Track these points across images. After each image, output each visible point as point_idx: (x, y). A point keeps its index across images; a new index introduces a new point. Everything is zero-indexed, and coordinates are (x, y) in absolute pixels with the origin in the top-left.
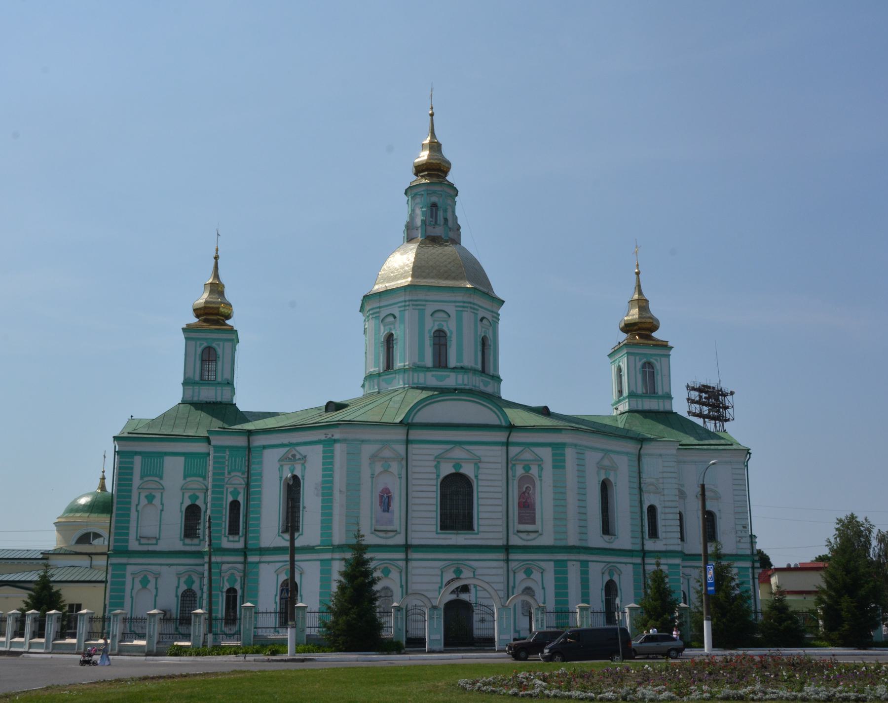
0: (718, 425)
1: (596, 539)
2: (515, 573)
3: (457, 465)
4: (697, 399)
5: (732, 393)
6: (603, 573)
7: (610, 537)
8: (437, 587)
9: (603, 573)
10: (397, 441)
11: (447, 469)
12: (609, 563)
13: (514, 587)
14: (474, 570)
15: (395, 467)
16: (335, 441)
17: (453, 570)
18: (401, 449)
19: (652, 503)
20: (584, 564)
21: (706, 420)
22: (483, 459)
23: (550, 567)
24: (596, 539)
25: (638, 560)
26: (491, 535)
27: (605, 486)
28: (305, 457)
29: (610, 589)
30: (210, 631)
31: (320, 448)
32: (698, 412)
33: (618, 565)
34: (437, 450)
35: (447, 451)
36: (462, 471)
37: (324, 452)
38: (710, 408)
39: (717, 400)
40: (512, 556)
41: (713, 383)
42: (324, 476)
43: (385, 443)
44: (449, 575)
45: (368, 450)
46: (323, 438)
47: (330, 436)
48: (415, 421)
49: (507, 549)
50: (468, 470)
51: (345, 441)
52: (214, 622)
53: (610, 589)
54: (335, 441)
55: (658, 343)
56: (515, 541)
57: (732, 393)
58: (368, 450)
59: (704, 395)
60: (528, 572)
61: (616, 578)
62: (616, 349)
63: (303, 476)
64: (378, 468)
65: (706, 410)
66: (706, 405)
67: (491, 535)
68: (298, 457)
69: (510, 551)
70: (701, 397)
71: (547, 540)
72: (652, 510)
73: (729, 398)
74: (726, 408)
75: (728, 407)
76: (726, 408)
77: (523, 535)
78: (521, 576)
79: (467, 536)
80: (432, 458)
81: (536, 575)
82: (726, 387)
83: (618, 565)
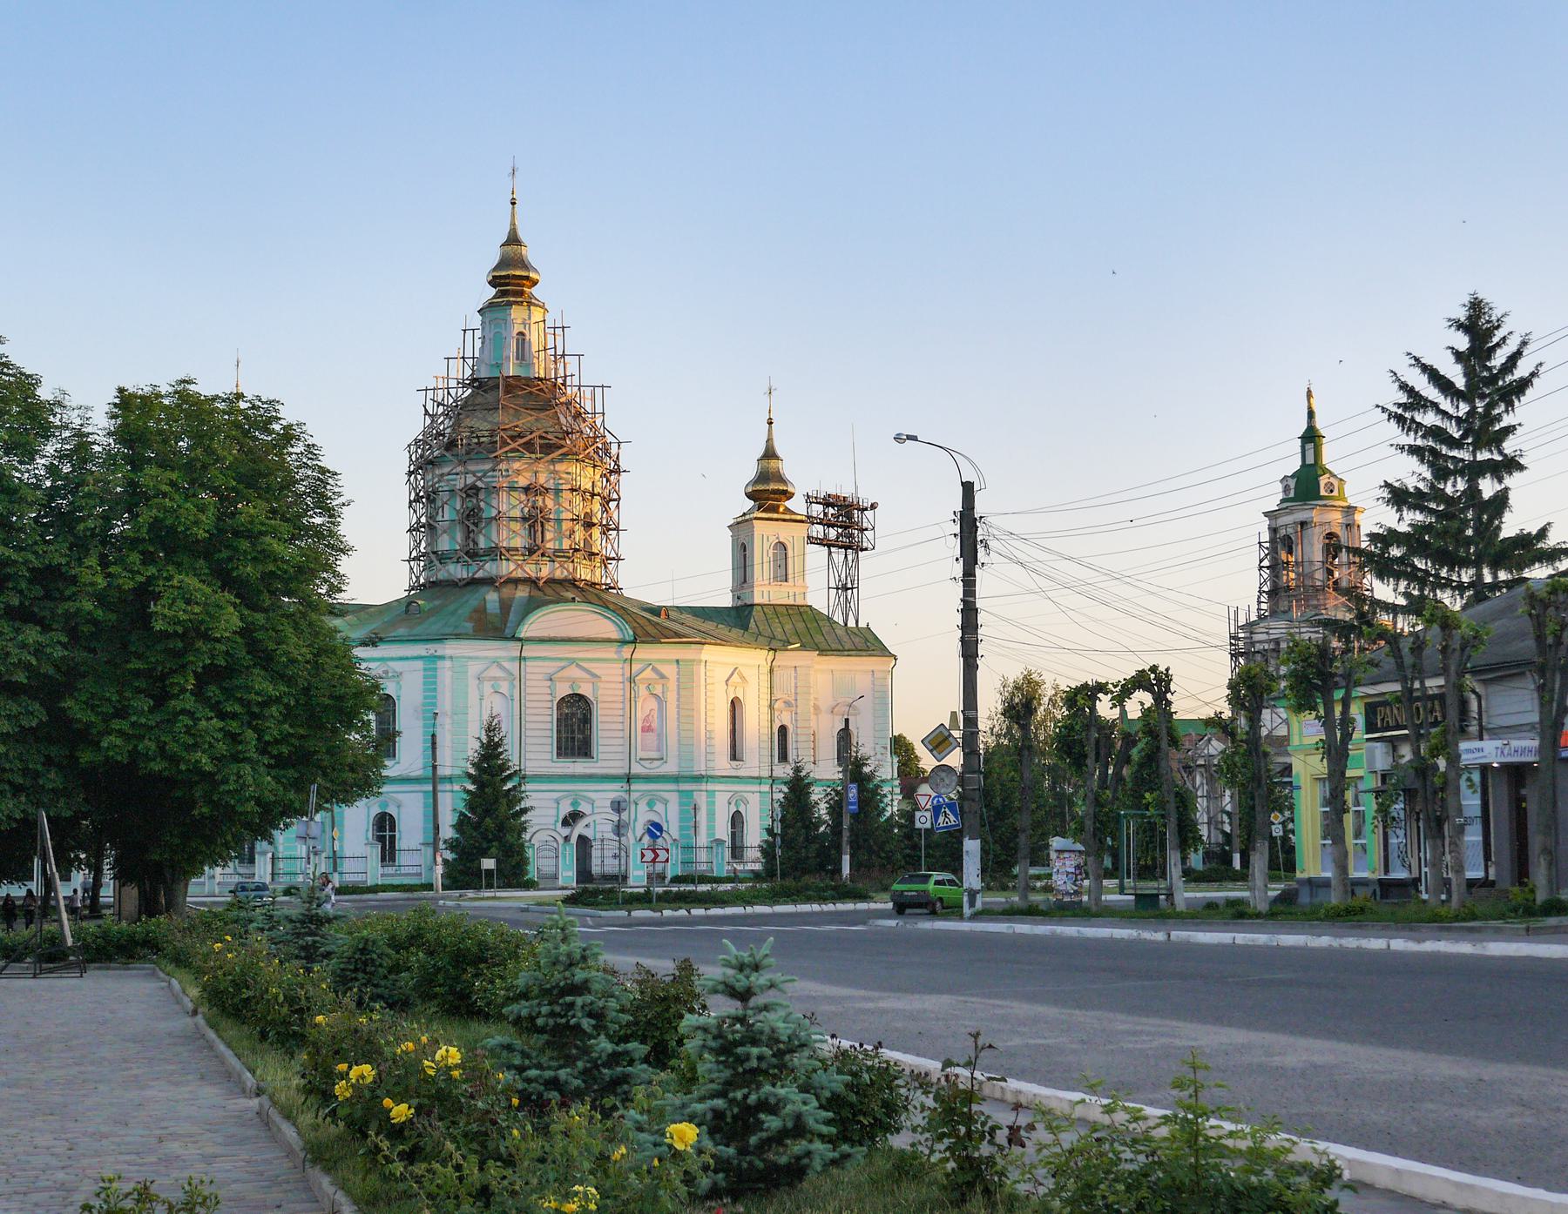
0: (850, 558)
1: (723, 764)
2: (636, 804)
3: (573, 682)
4: (822, 516)
5: (873, 507)
6: (730, 804)
7: (737, 763)
8: (552, 820)
9: (730, 804)
10: (513, 659)
11: (563, 690)
12: (737, 792)
13: (635, 820)
14: (592, 802)
15: (504, 687)
16: (442, 658)
17: (569, 802)
18: (513, 667)
19: (785, 723)
20: (711, 793)
21: (833, 549)
22: (603, 678)
23: (673, 798)
24: (723, 764)
25: (766, 788)
26: (611, 764)
27: (735, 704)
28: (401, 673)
29: (737, 820)
30: (335, 870)
31: (419, 664)
32: (821, 536)
33: (745, 795)
34: (550, 667)
35: (563, 668)
36: (580, 692)
37: (425, 670)
38: (840, 531)
39: (850, 516)
40: (633, 787)
41: (846, 491)
42: (425, 698)
43: (496, 662)
44: (566, 809)
45: (474, 668)
46: (424, 653)
47: (432, 651)
48: (528, 635)
49: (629, 778)
50: (585, 690)
51: (451, 657)
52: (338, 860)
53: (737, 820)
54: (442, 658)
55: (794, 517)
56: (637, 769)
57: (873, 507)
58: (474, 668)
59: (831, 511)
60: (650, 804)
61: (742, 809)
62: (740, 519)
63: (398, 696)
64: (487, 688)
65: (832, 533)
66: (833, 526)
67: (611, 764)
68: (390, 675)
69: (631, 781)
70: (825, 514)
71: (670, 768)
72: (783, 730)
73: (868, 513)
74: (862, 530)
75: (866, 529)
76: (862, 530)
77: (646, 764)
78: (643, 807)
79: (586, 765)
80: (547, 677)
81: (659, 807)
82: (866, 498)
83: (745, 795)
